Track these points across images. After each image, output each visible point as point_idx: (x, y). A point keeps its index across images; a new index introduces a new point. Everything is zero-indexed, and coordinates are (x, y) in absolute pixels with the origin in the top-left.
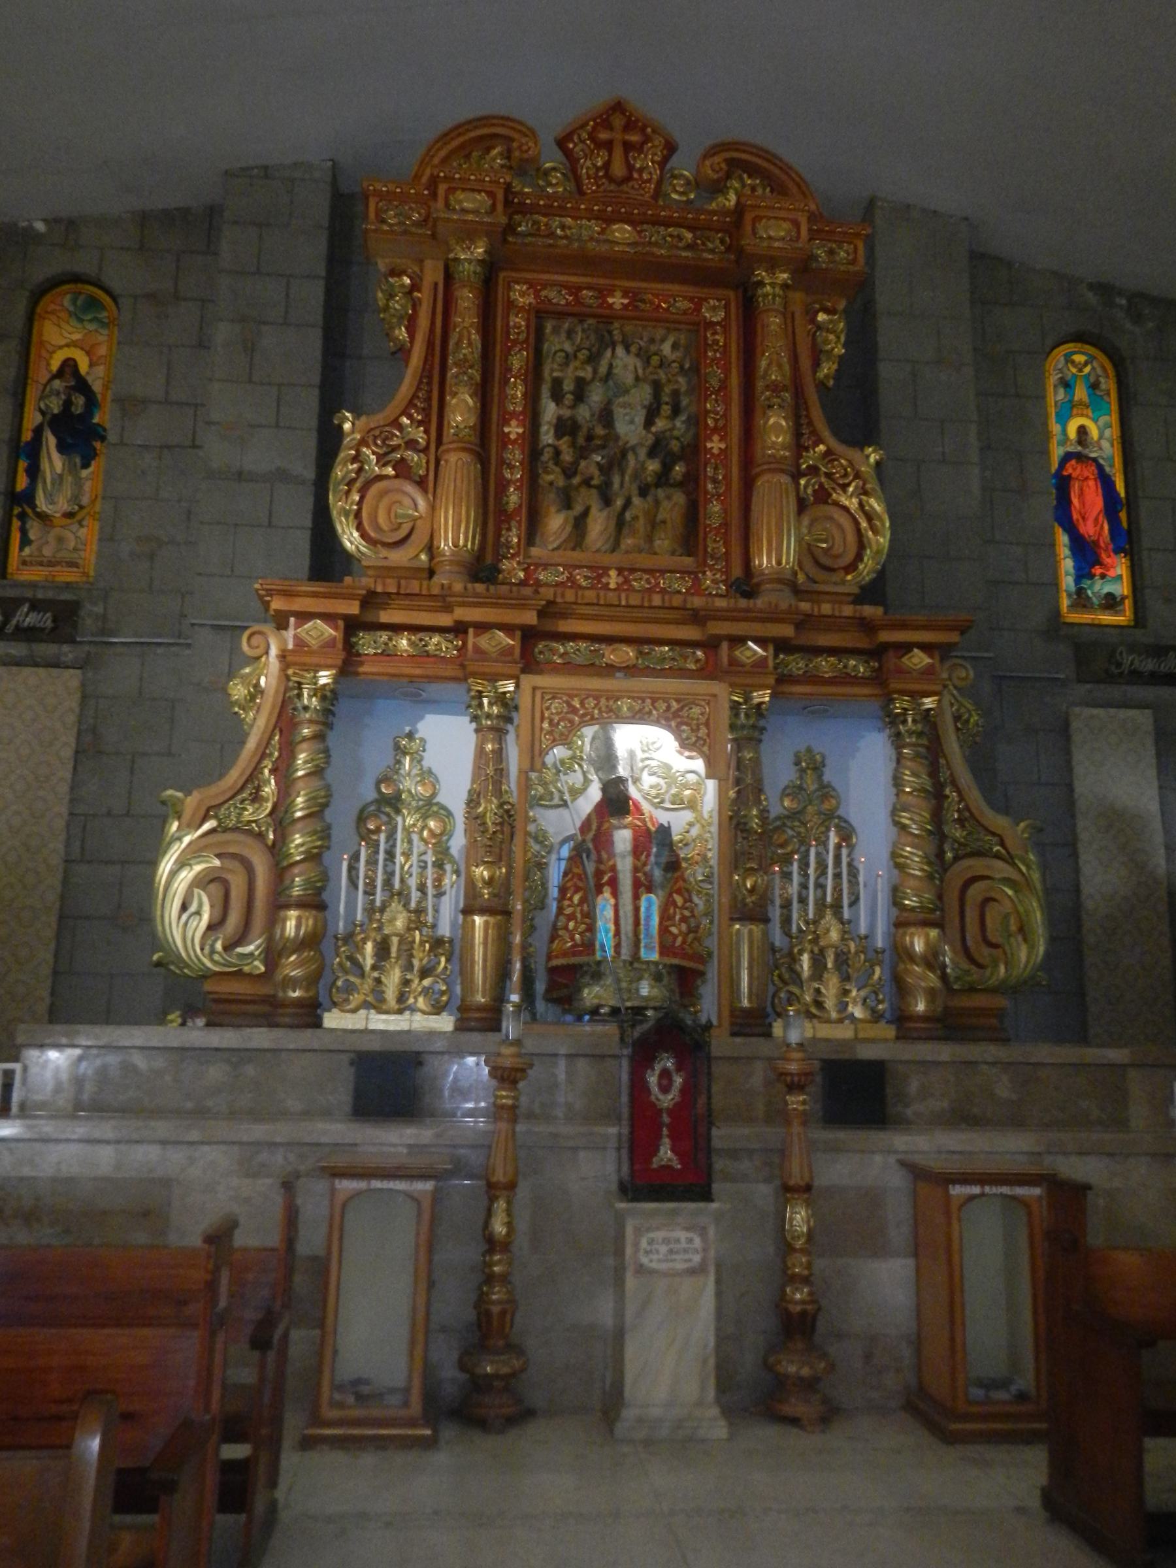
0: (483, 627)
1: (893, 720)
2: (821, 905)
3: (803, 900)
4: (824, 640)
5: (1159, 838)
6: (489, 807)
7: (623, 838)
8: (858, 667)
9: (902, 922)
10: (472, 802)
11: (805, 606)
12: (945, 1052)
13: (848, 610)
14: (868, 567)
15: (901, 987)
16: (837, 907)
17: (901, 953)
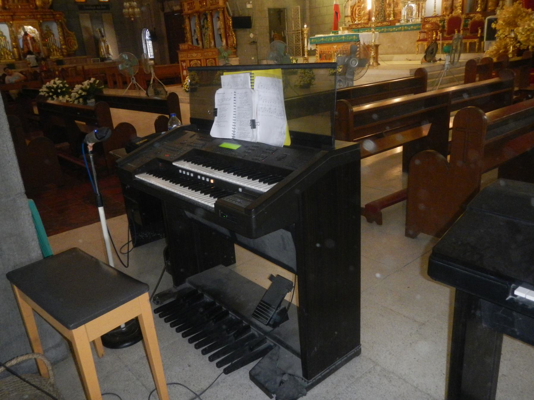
0: (6, 16)
1: (56, 23)
2: (52, 44)
3: (50, 43)
4: (47, 14)
5: (92, 31)
6: (13, 36)
7: (28, 38)
8: (52, 16)
9: (62, 45)
10: (10, 36)
11: (44, 10)
12: (68, 58)
13: (49, 10)
14: (50, 3)
15: (62, 52)
16: (54, 44)
17: (61, 49)
